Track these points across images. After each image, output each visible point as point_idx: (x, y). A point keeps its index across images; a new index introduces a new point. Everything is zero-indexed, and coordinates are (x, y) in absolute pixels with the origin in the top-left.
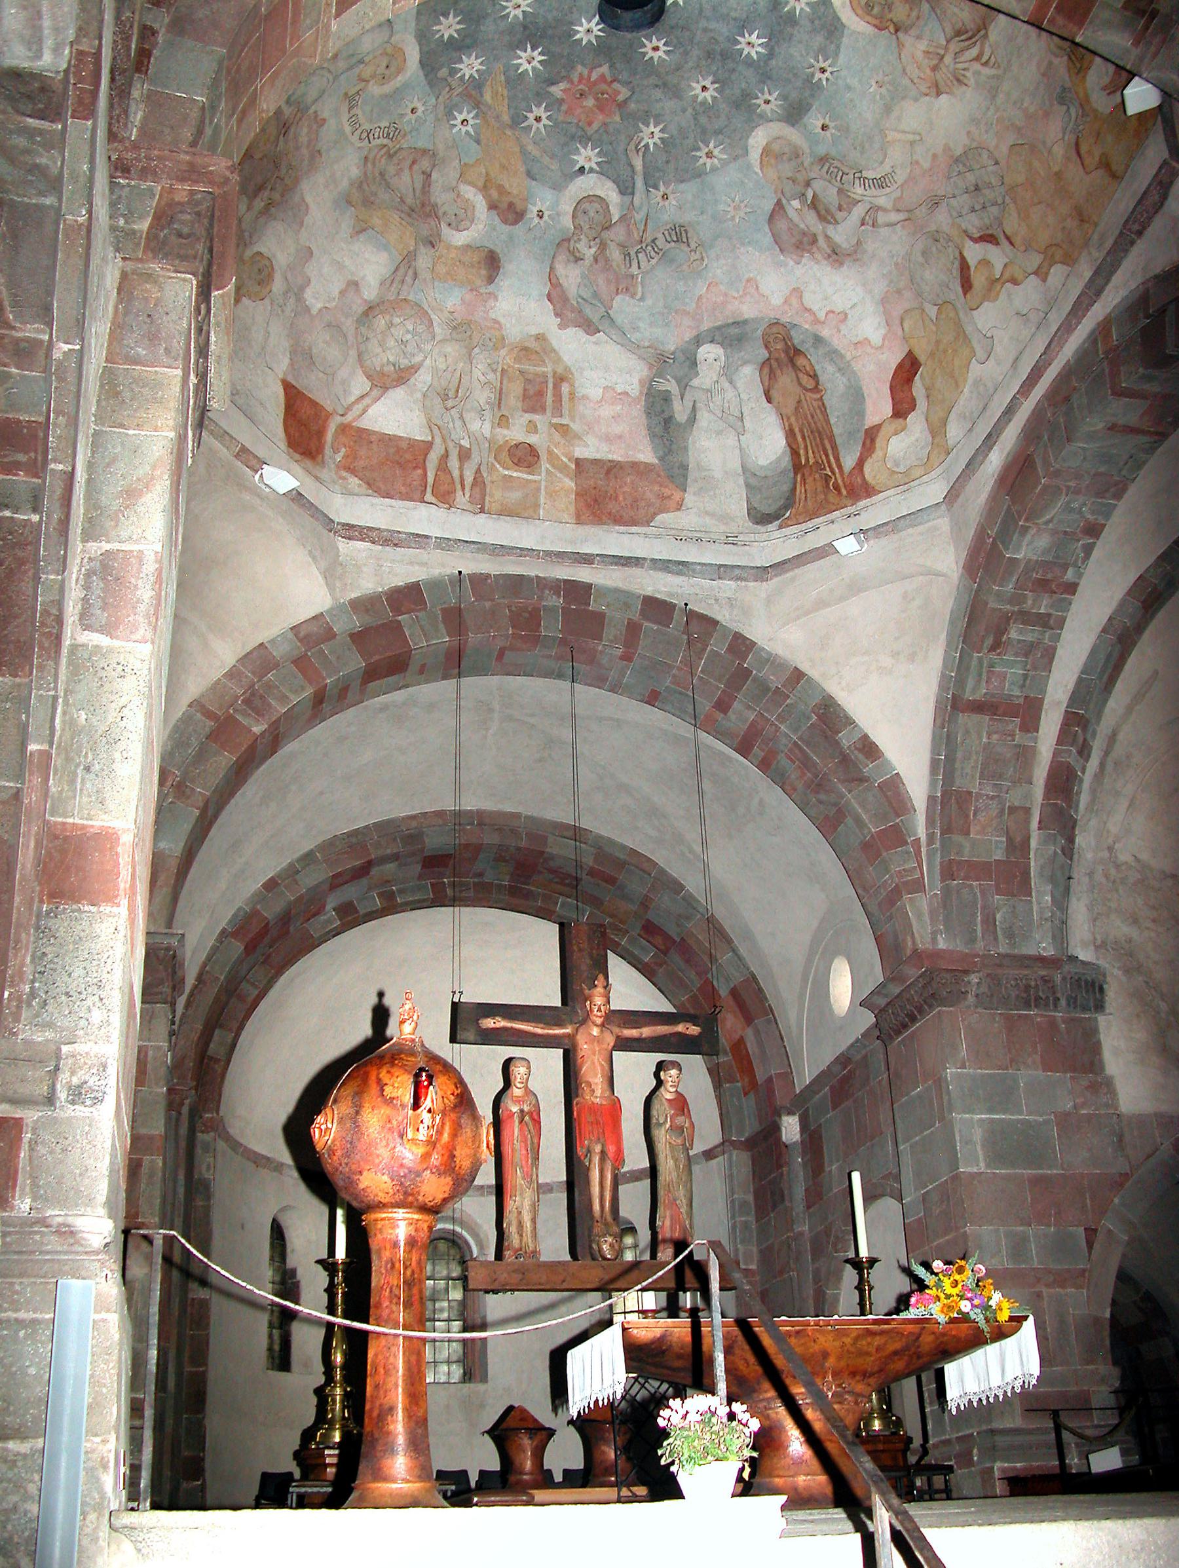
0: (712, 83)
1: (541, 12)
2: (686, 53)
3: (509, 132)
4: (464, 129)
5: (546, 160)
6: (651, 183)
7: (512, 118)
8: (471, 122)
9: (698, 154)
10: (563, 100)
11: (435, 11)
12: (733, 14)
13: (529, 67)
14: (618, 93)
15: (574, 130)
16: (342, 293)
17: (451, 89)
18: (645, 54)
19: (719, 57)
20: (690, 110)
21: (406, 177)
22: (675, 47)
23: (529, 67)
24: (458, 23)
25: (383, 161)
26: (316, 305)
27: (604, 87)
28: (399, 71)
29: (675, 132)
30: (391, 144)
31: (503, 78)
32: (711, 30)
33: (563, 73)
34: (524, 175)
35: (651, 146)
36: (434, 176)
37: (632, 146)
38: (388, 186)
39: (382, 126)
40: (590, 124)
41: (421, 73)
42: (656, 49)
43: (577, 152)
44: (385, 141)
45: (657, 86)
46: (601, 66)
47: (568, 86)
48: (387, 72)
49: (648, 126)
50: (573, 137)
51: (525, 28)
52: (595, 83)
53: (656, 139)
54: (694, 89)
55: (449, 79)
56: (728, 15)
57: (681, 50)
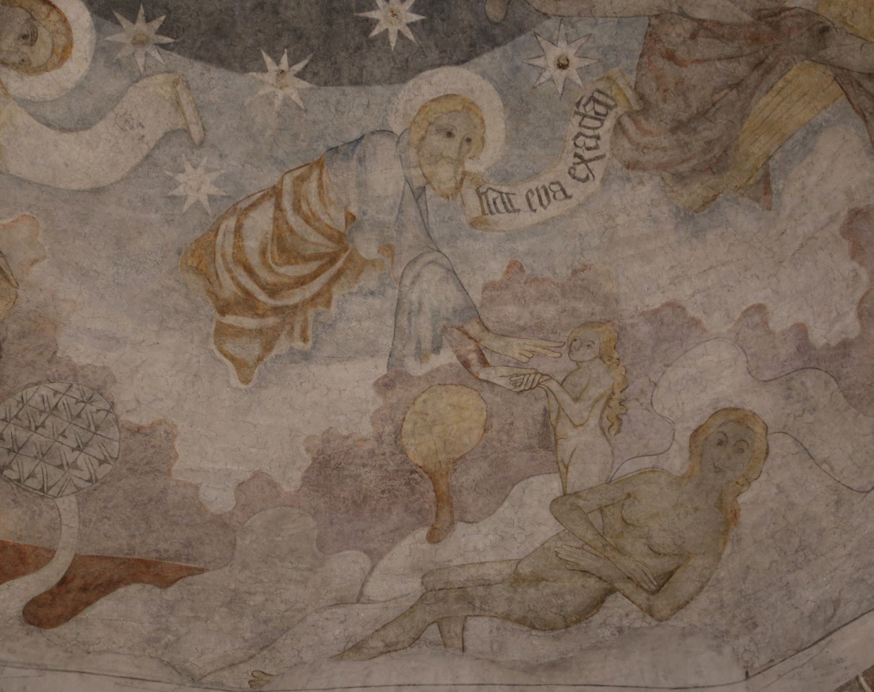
11: (358, 48)
16: (857, 252)
21: (693, 74)
25: (650, 125)
26: (851, 326)
28: (470, 108)
30: (620, 110)
36: (703, 14)
38: (703, 114)
39: (576, 130)
41: (485, 60)
44: (609, 123)
48: (459, 136)
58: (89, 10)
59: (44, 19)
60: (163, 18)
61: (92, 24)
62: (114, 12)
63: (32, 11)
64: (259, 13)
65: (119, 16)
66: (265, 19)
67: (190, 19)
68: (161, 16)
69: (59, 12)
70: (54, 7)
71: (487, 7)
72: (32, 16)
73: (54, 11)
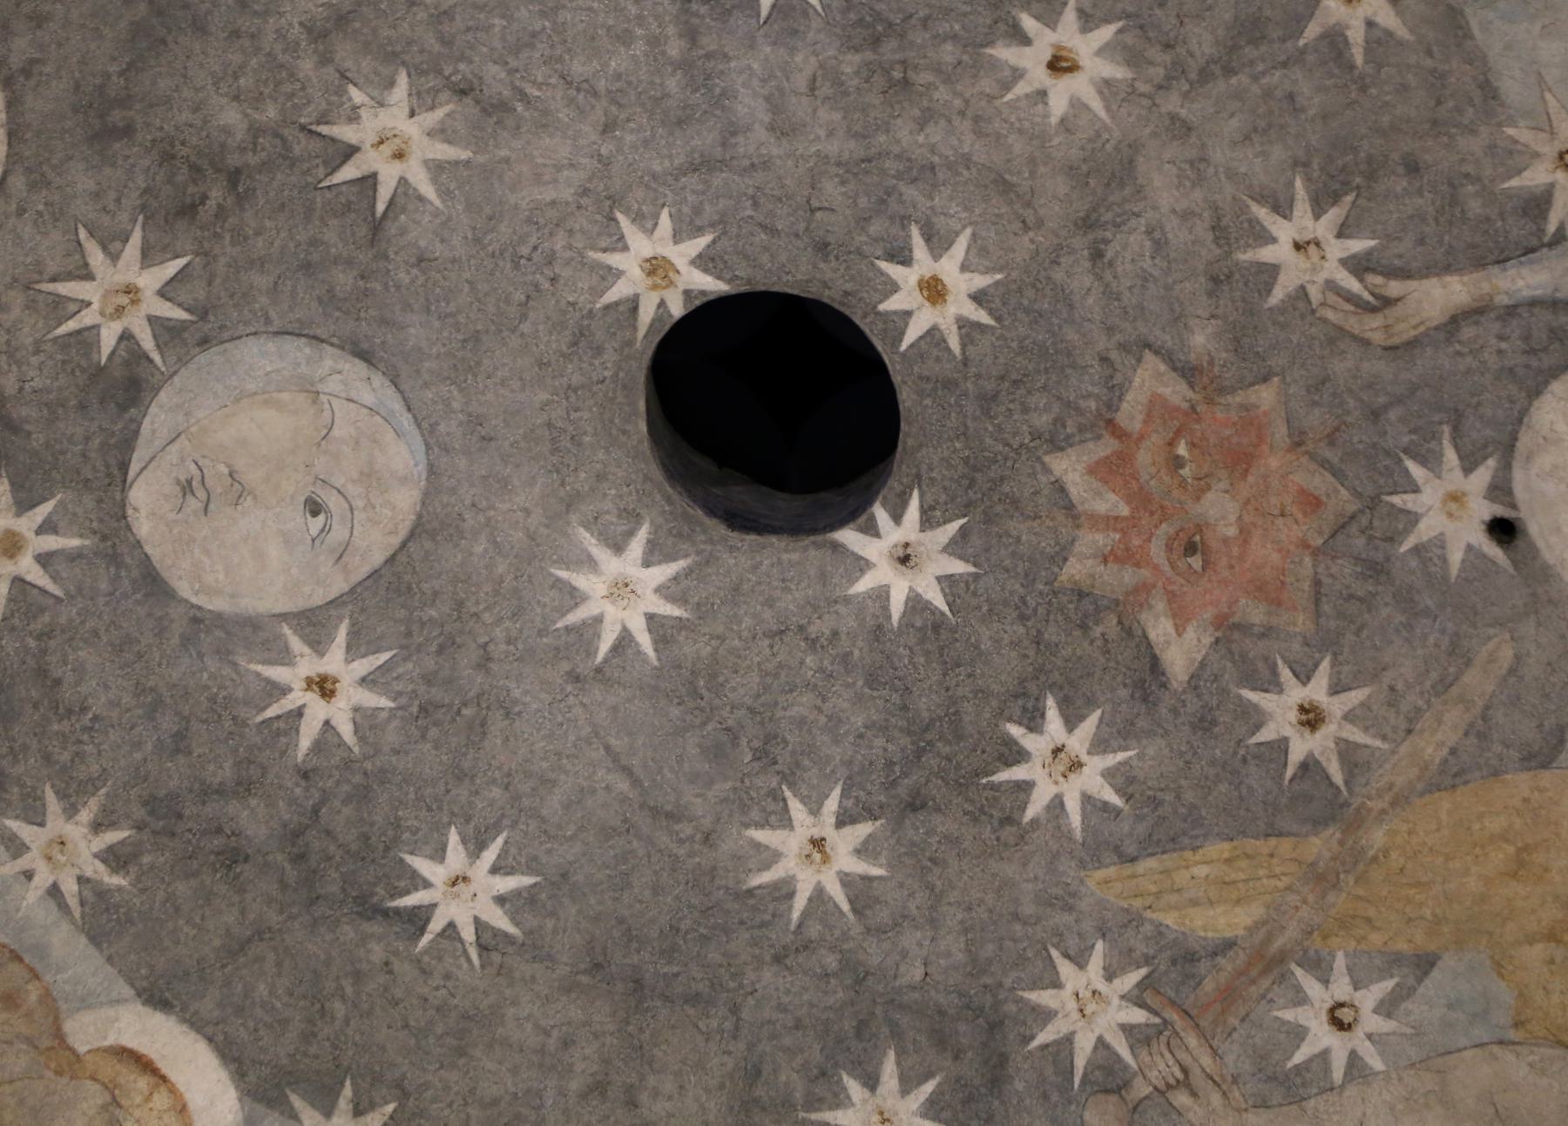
0: (1025, 40)
1: (837, 753)
2: (923, 173)
3: (1377, 837)
4: (1371, 1022)
5: (1478, 682)
6: (1518, 230)
7: (1319, 823)
8: (1341, 989)
9: (1356, 35)
10: (1220, 622)
12: (675, 49)
13: (1096, 765)
14: (1156, 407)
15: (1345, 569)
17: (1185, 1083)
18: (963, 323)
19: (890, 50)
20: (1172, 103)
22: (904, 221)
23: (1096, 765)
24: (871, 1082)
27: (1144, 457)
29: (1278, 153)
31: (1151, 863)
32: (775, 105)
33: (1110, 625)
34: (1546, 778)
35: (1358, 246)
37: (1372, 326)
40: (1312, 503)
42: (934, 290)
43: (1426, 553)
45: (1097, 255)
46: (1060, 488)
47: (1160, 605)
49: (1271, 272)
50: (1376, 570)
51: (916, 804)
52: (1141, 499)
53: (1323, 228)
54: (1077, 105)
55: (1141, 1089)
56: (684, 65)
57: (910, 192)
58: (237, 1088)
59: (138, 1106)
60: (390, 1108)
61: (240, 1117)
62: (288, 1092)
63: (115, 1087)
64: (595, 1103)
65: (297, 1102)
66: (608, 1117)
67: (447, 1112)
68: (387, 1103)
69: (173, 1090)
70: (164, 1079)
71: (1087, 1116)
72: (114, 1097)
73: (163, 1089)
